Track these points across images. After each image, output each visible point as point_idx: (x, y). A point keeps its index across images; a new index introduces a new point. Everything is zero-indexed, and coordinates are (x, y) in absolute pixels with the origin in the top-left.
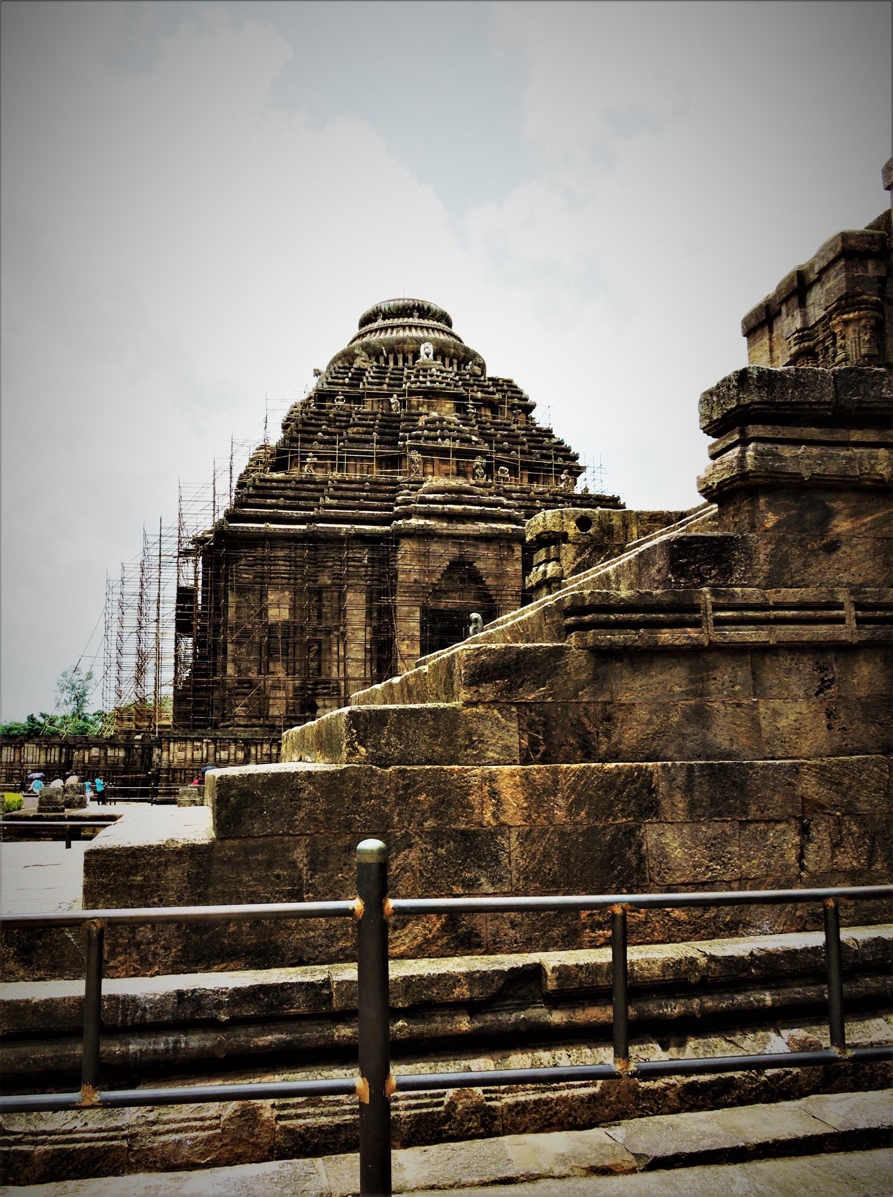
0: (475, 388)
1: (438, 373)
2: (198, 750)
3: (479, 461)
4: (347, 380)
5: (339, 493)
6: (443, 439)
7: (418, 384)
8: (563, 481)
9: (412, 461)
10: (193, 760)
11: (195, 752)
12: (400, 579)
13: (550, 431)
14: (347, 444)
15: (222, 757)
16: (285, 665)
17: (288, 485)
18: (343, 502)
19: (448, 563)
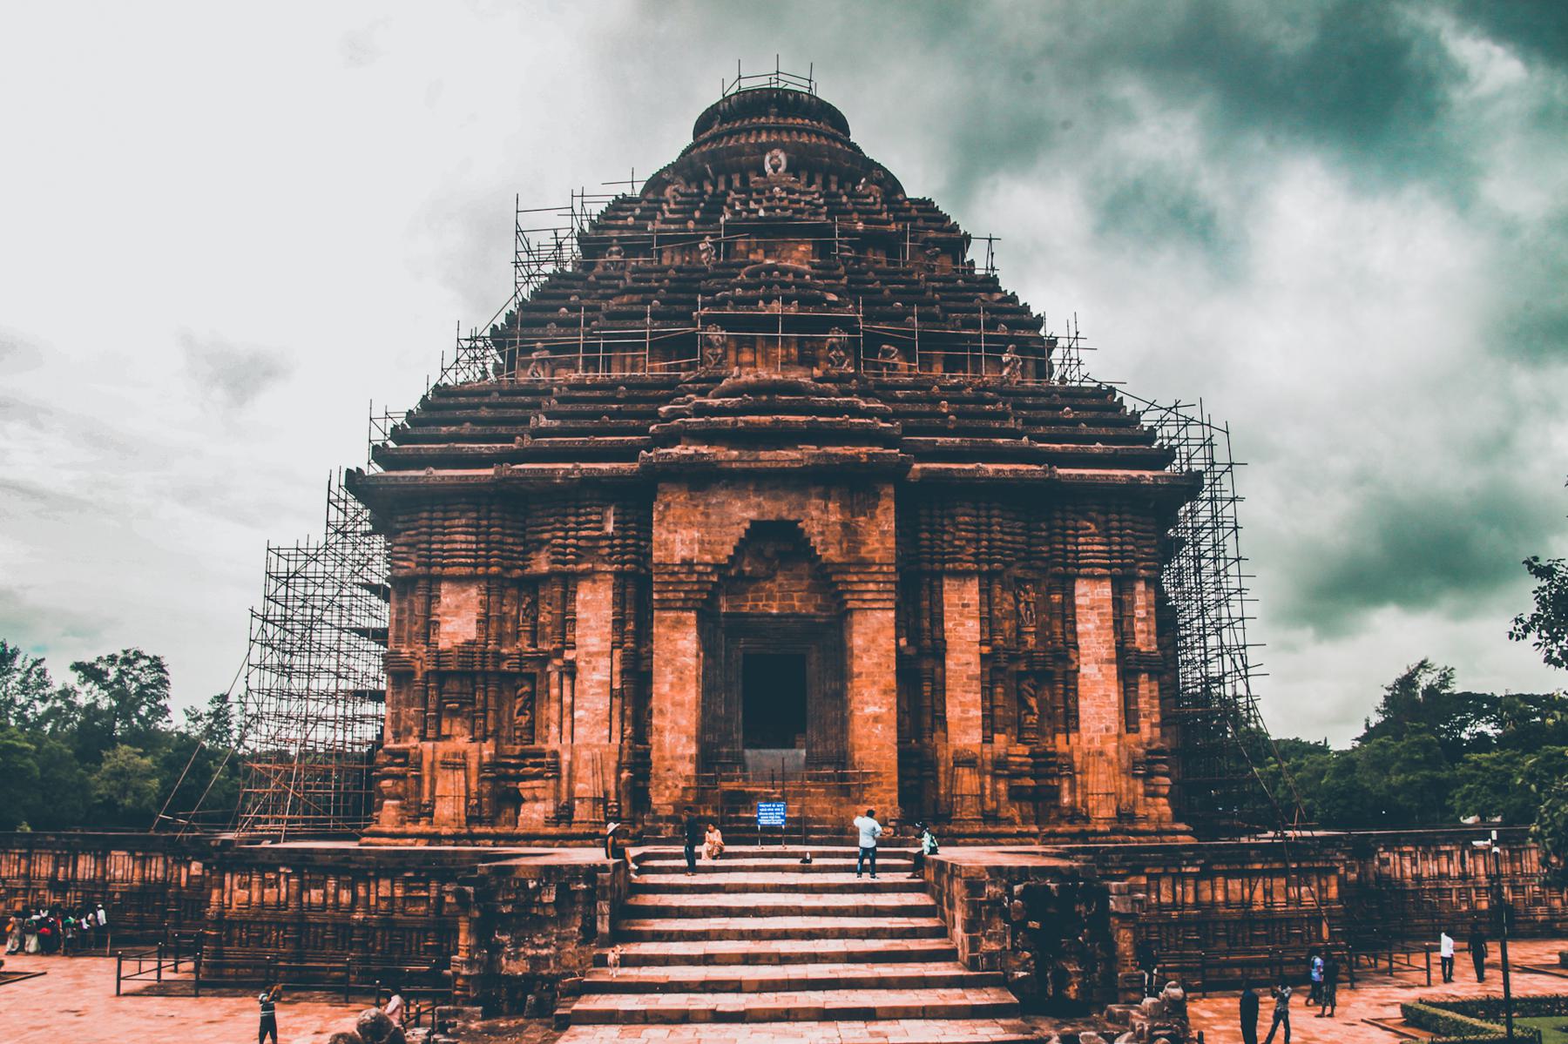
0: (855, 216)
1: (784, 195)
2: (271, 886)
3: (834, 336)
4: (631, 220)
5: (569, 407)
6: (768, 301)
7: (744, 214)
8: (1007, 364)
9: (709, 344)
10: (262, 905)
11: (267, 891)
12: (655, 560)
13: (995, 280)
14: (603, 322)
15: (313, 899)
16: (468, 724)
17: (487, 400)
18: (570, 424)
19: (747, 525)
